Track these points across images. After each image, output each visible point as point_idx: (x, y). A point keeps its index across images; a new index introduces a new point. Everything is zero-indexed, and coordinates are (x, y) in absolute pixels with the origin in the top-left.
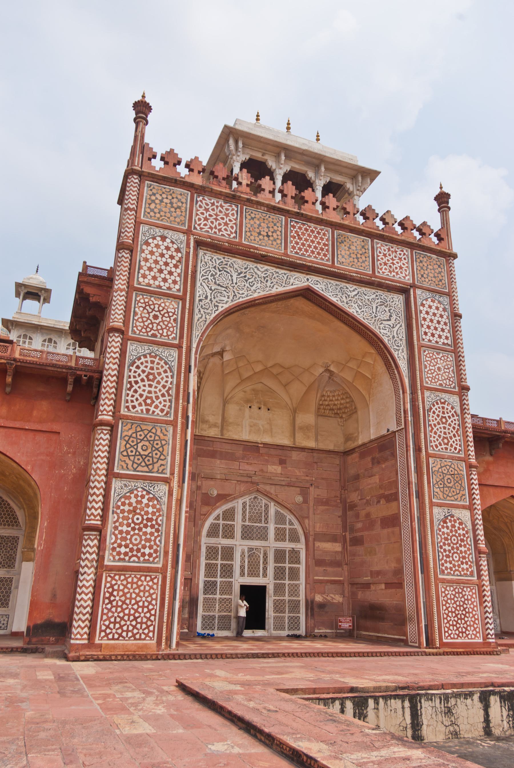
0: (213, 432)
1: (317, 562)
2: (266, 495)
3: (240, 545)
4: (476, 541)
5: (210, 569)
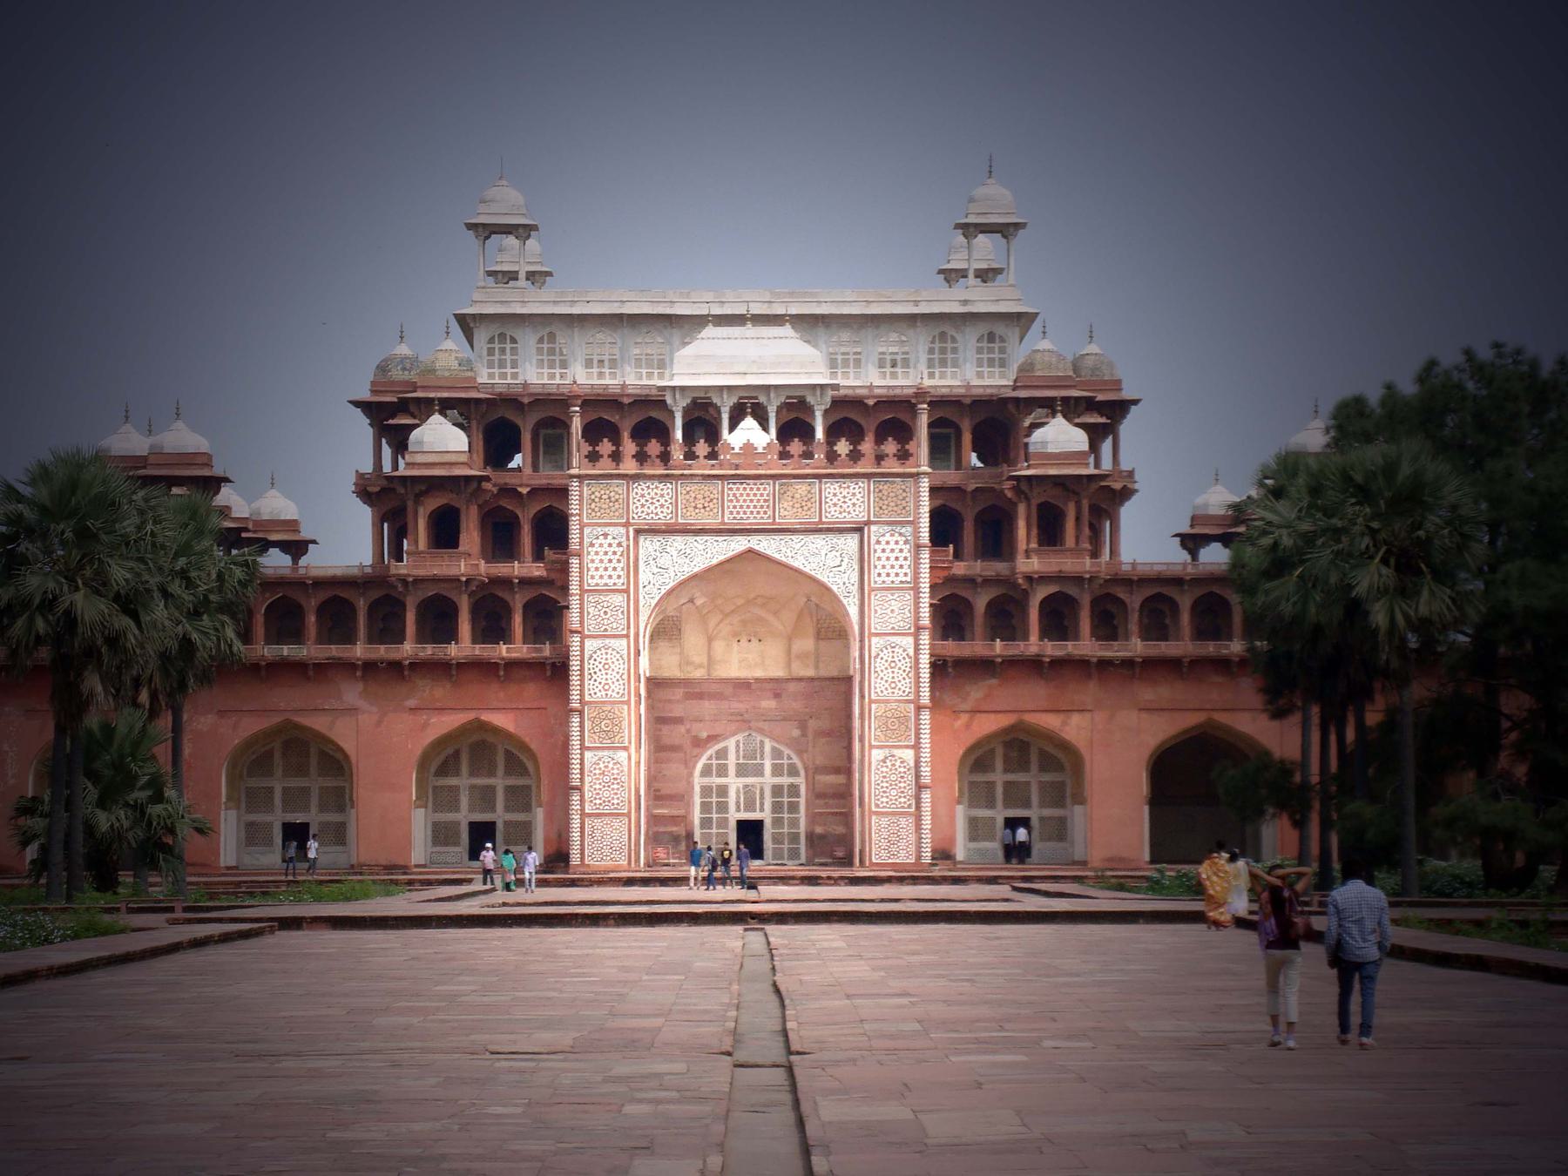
0: (699, 674)
1: (817, 795)
2: (761, 731)
3: (734, 783)
4: (918, 776)
5: (706, 807)
